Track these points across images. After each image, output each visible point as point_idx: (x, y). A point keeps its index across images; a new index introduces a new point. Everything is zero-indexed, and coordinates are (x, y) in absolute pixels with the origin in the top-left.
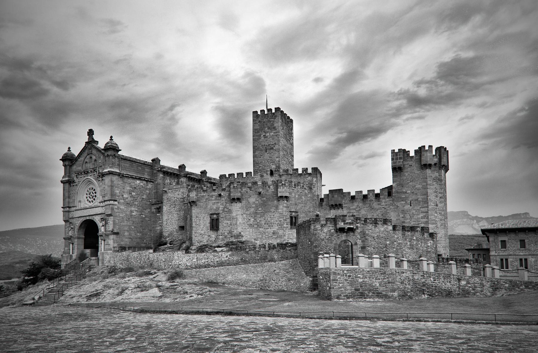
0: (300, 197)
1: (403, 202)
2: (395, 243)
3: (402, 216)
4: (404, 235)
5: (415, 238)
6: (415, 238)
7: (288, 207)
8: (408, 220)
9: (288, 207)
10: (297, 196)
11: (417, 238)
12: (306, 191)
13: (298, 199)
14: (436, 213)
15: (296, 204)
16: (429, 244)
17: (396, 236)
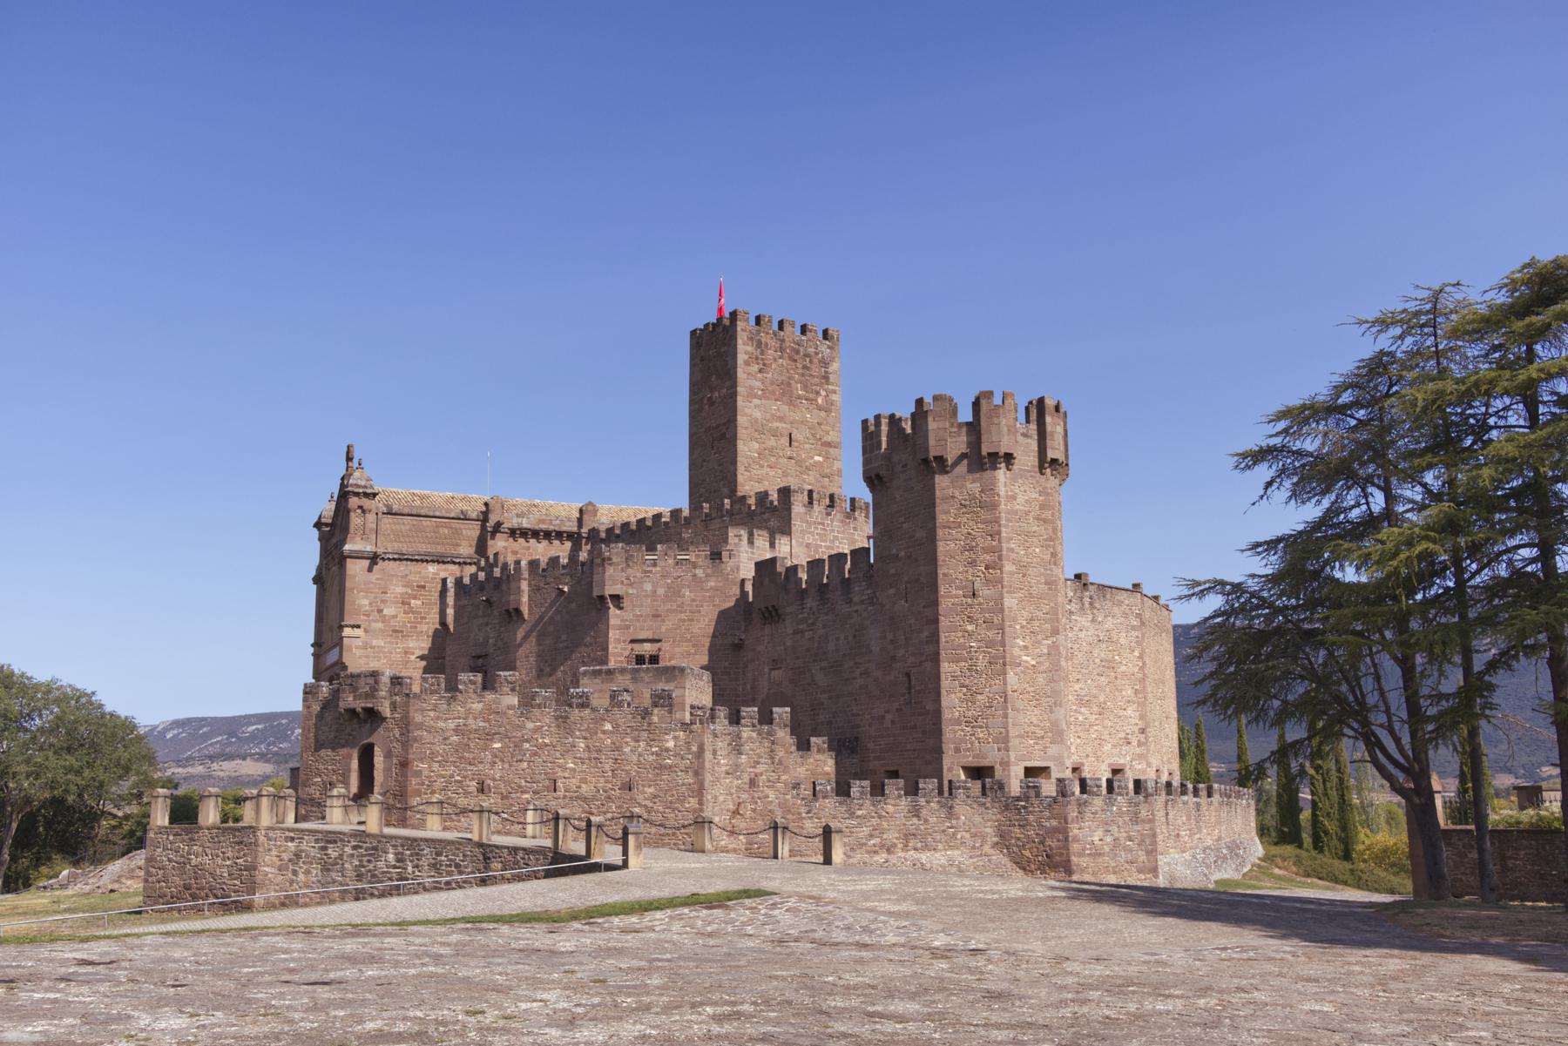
0: (674, 592)
1: (892, 591)
2: (527, 745)
3: (890, 636)
4: (562, 720)
5: (608, 727)
6: (608, 727)
7: (628, 627)
8: (901, 652)
9: (628, 627)
10: (661, 591)
11: (616, 726)
12: (699, 572)
13: (667, 598)
14: (971, 619)
15: (656, 616)
16: (671, 744)
17: (530, 725)
